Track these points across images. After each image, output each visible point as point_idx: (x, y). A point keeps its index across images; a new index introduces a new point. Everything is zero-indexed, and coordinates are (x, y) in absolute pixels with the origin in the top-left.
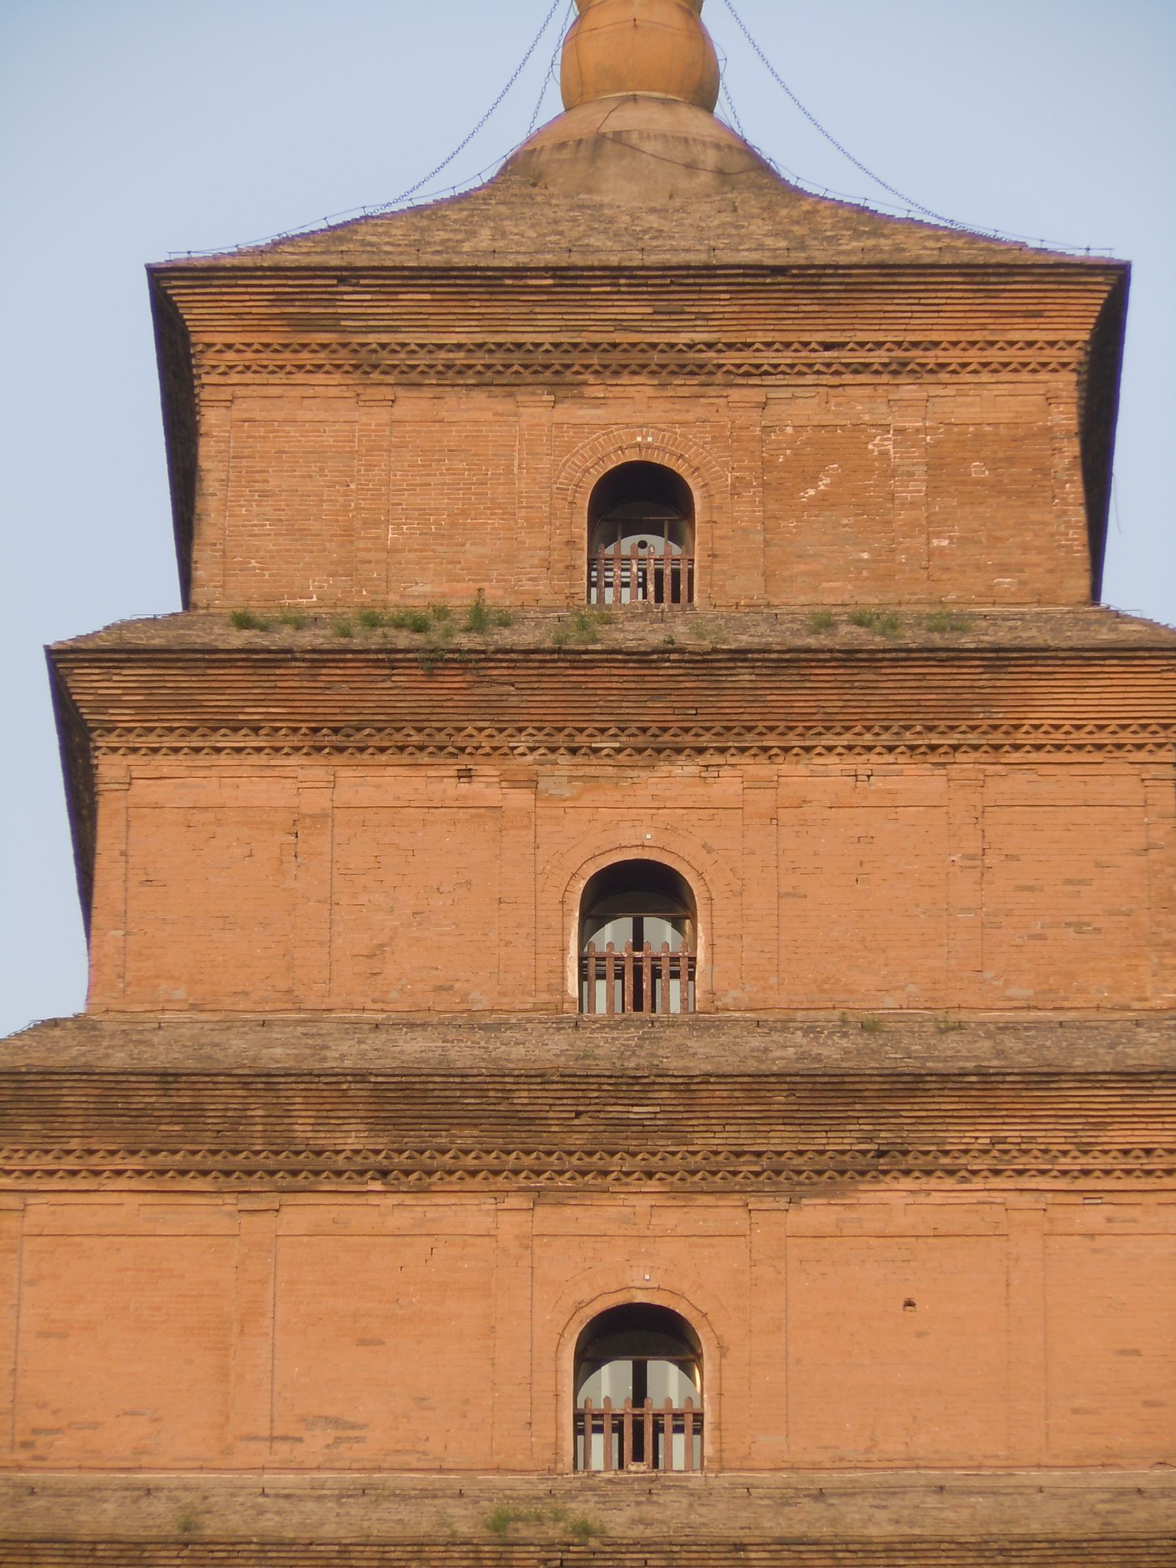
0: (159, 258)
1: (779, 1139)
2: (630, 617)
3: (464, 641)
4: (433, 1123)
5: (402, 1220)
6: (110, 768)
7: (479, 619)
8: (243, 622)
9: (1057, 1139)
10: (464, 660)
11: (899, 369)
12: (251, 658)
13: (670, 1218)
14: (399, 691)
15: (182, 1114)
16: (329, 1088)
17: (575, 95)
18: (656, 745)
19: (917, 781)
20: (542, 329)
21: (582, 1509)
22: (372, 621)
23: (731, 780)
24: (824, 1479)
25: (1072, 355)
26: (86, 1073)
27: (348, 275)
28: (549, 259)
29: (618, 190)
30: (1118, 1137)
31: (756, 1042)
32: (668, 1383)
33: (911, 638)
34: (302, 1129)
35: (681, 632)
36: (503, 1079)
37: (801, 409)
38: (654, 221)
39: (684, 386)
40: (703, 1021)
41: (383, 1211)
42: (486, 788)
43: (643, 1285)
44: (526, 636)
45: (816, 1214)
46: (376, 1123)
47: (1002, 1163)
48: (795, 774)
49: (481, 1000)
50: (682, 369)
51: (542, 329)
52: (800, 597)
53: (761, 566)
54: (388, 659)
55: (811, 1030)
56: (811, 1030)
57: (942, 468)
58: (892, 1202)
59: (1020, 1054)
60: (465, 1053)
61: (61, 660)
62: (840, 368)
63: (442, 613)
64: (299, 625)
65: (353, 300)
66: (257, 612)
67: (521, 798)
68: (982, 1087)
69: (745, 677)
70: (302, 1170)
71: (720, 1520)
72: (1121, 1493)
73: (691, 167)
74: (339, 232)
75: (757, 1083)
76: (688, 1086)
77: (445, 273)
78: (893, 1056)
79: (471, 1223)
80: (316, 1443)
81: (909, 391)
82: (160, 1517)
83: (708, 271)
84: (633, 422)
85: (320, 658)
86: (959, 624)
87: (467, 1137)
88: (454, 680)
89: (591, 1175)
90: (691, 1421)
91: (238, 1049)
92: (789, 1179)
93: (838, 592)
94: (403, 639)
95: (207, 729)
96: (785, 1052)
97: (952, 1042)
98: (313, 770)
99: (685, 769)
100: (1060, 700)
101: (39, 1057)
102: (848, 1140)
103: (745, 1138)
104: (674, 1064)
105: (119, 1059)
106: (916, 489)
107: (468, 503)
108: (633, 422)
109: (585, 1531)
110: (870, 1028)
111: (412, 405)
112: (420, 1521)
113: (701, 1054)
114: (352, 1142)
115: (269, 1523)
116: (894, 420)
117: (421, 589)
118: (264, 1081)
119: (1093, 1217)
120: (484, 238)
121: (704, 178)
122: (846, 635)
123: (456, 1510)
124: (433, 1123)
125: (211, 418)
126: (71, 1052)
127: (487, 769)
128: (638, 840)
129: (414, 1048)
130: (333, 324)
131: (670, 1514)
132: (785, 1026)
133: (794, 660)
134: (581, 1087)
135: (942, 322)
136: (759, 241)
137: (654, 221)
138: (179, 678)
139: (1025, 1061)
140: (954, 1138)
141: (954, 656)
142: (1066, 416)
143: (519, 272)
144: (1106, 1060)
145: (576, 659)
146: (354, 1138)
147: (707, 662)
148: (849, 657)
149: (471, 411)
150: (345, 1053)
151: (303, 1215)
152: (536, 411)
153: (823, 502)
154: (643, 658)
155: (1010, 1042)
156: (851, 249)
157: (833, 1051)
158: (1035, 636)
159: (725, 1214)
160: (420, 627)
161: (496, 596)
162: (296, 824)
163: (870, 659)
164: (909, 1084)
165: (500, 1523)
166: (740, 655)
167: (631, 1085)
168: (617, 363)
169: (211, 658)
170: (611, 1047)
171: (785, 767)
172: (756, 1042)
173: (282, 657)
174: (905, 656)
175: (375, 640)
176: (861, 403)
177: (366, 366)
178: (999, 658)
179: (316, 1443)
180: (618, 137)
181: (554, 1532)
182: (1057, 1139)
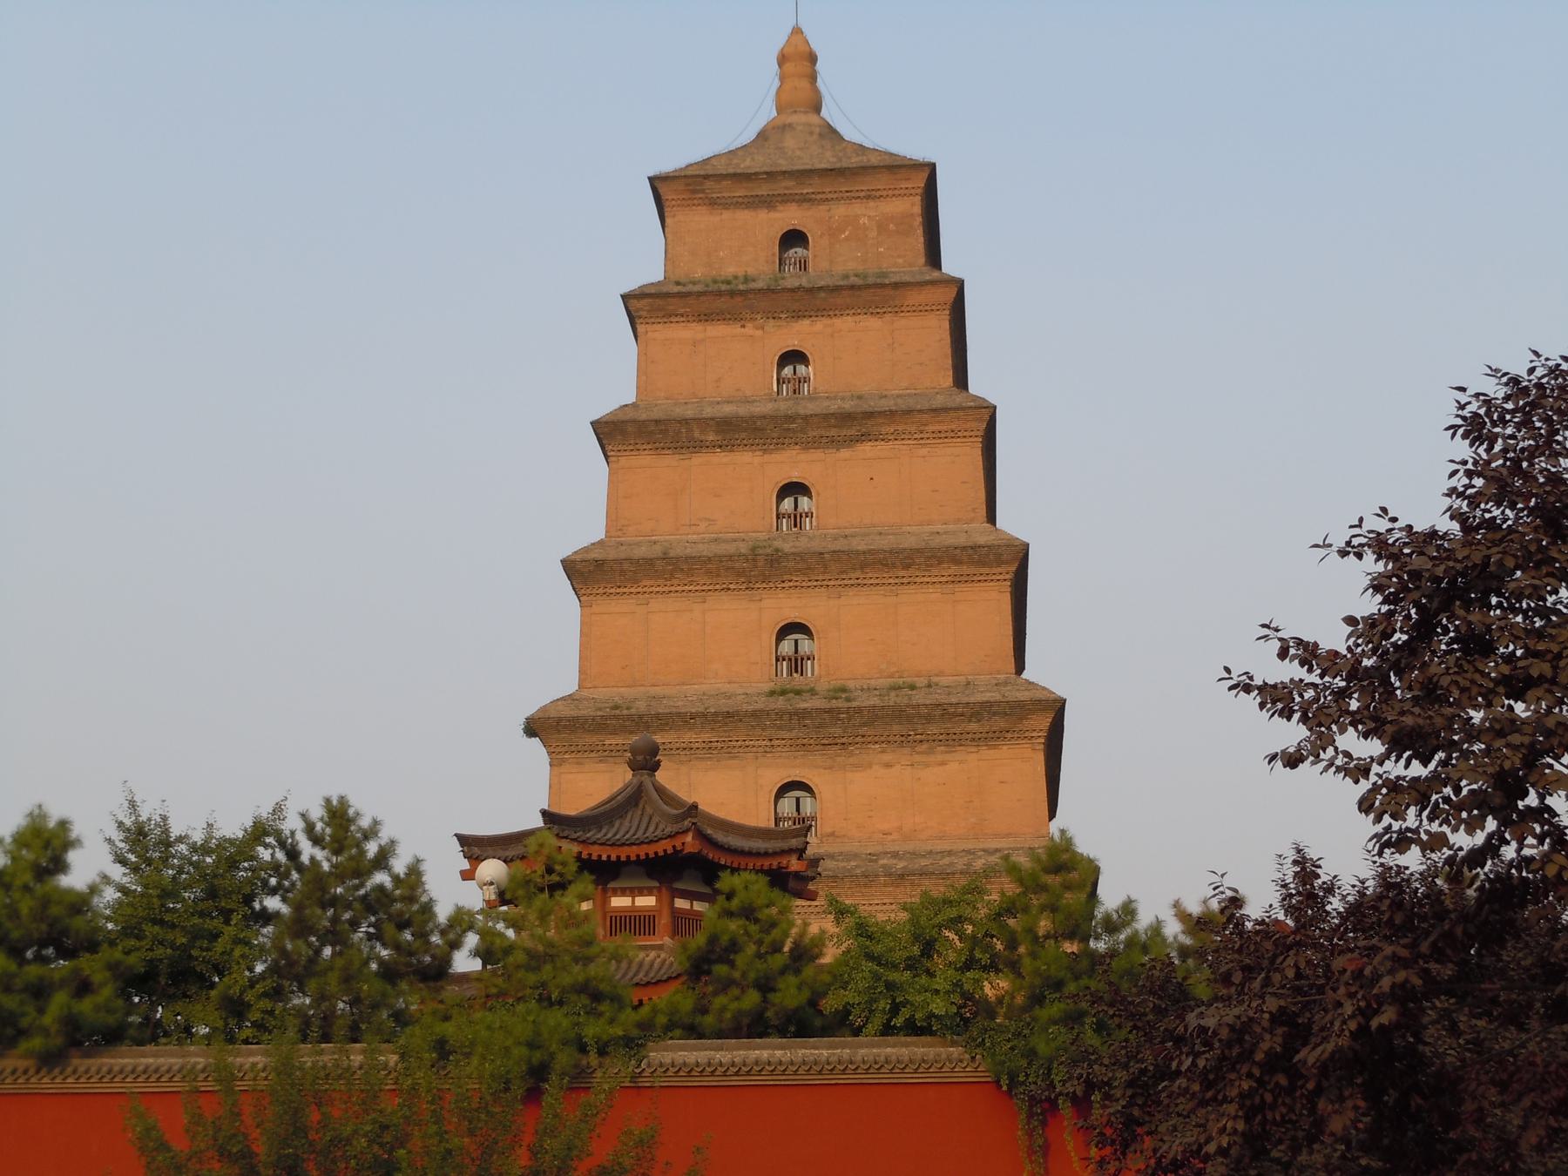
0: (653, 171)
1: (834, 432)
2: (792, 279)
3: (741, 287)
4: (737, 431)
5: (725, 460)
6: (640, 329)
7: (746, 280)
8: (678, 283)
9: (913, 429)
10: (742, 293)
11: (868, 197)
12: (680, 295)
13: (804, 456)
14: (722, 303)
15: (661, 432)
16: (704, 423)
17: (780, 110)
18: (797, 315)
19: (873, 323)
20: (763, 190)
21: (778, 544)
22: (715, 282)
23: (820, 325)
24: (847, 532)
25: (919, 191)
26: (634, 421)
27: (706, 177)
28: (765, 169)
29: (790, 142)
30: (930, 428)
31: (826, 403)
32: (804, 503)
33: (871, 280)
34: (697, 434)
35: (804, 282)
36: (752, 419)
37: (840, 211)
38: (798, 153)
39: (806, 205)
40: (812, 398)
41: (721, 457)
42: (749, 329)
43: (795, 476)
44: (760, 285)
45: (845, 453)
46: (717, 432)
48: (837, 322)
49: (748, 393)
50: (805, 200)
51: (763, 190)
52: (839, 269)
53: (829, 259)
54: (720, 294)
55: (843, 399)
56: (843, 399)
57: (881, 227)
58: (866, 449)
59: (902, 405)
60: (743, 411)
61: (624, 297)
63: (736, 277)
64: (694, 283)
65: (708, 184)
66: (682, 280)
67: (759, 333)
68: (891, 415)
69: (823, 295)
70: (697, 446)
71: (816, 545)
72: (932, 533)
73: (811, 133)
74: (706, 161)
75: (826, 417)
76: (806, 418)
77: (735, 175)
78: (865, 407)
79: (745, 460)
80: (703, 526)
81: (872, 204)
82: (657, 551)
83: (812, 172)
84: (790, 217)
85: (700, 294)
86: (884, 275)
87: (743, 435)
88: (739, 299)
89: (780, 444)
90: (809, 514)
91: (679, 412)
92: (835, 443)
93: (851, 266)
94: (724, 287)
95: (668, 316)
96: (834, 407)
97: (883, 401)
98: (698, 327)
99: (806, 322)
100: (915, 297)
101: (621, 417)
102: (853, 432)
103: (823, 433)
104: (802, 412)
105: (644, 417)
106: (874, 234)
107: (742, 243)
108: (790, 217)
109: (777, 550)
110: (860, 397)
111: (726, 215)
112: (730, 549)
113: (811, 408)
114: (711, 437)
115: (688, 551)
116: (866, 213)
117: (730, 270)
118: (685, 422)
119: (924, 451)
120: (748, 162)
121: (815, 137)
122: (854, 280)
123: (742, 545)
124: (737, 431)
125: (668, 221)
126: (631, 415)
127: (749, 325)
128: (793, 343)
129: (728, 409)
130: (703, 191)
131: (803, 544)
132: (835, 398)
133: (836, 289)
134: (773, 418)
135: (881, 182)
136: (828, 160)
137: (798, 153)
138: (659, 302)
139: (904, 407)
140: (884, 430)
141: (883, 286)
142: (917, 209)
143: (756, 174)
144: (926, 406)
145: (773, 291)
146: (711, 437)
147: (811, 291)
148: (852, 287)
149: (744, 215)
150: (708, 412)
151: (698, 459)
152: (763, 215)
153: (847, 239)
154: (793, 290)
155: (900, 401)
156: (855, 161)
157: (848, 406)
158: (907, 278)
159: (817, 455)
160: (728, 283)
161: (751, 271)
162: (695, 343)
163: (859, 288)
164: (870, 415)
165: (753, 549)
166: (821, 288)
167: (790, 418)
168: (786, 199)
169: (668, 295)
170: (783, 407)
171: (835, 320)
172: (826, 403)
173: (689, 294)
174: (868, 286)
175: (715, 287)
176: (857, 208)
177: (713, 203)
178: (896, 286)
179: (703, 526)
180: (790, 125)
181: (769, 551)
182: (913, 429)
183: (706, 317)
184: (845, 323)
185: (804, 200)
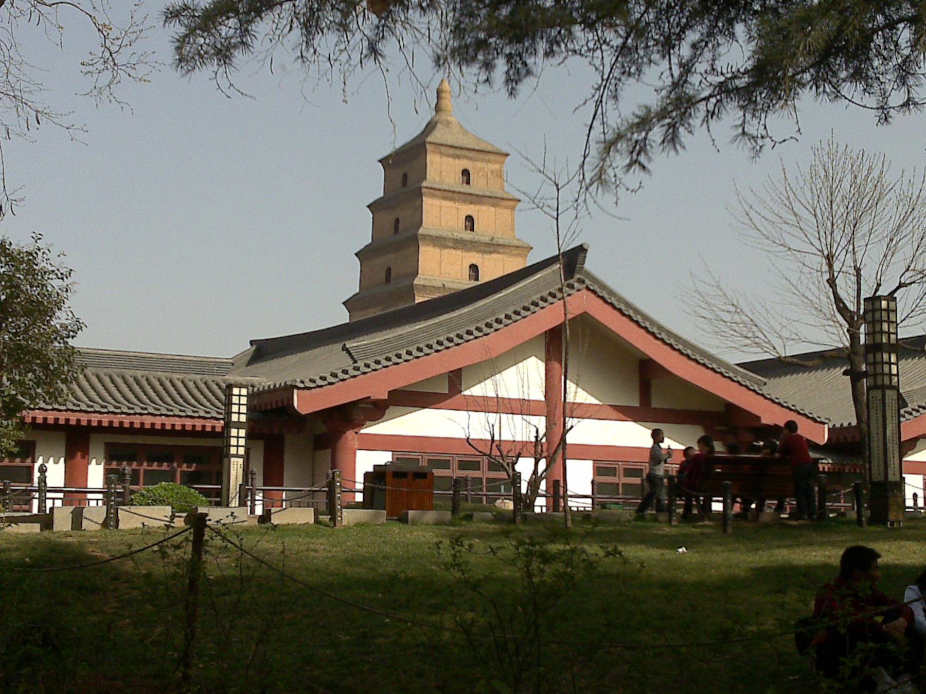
1: (486, 249)
4: (459, 244)
14: (450, 194)
19: (493, 209)
20: (458, 152)
23: (477, 207)
37: (479, 164)
41: (453, 252)
45: (488, 256)
47: (503, 253)
58: (495, 256)
62: (483, 161)
68: (504, 246)
95: (433, 196)
100: (505, 203)
111: (445, 159)
135: (492, 157)
146: (451, 244)
149: (451, 160)
150: (451, 236)
151: (446, 251)
152: (457, 161)
168: (464, 157)
176: (484, 165)
177: (441, 154)
178: (503, 199)
183: (445, 198)
184: (484, 208)
185: (470, 159)
